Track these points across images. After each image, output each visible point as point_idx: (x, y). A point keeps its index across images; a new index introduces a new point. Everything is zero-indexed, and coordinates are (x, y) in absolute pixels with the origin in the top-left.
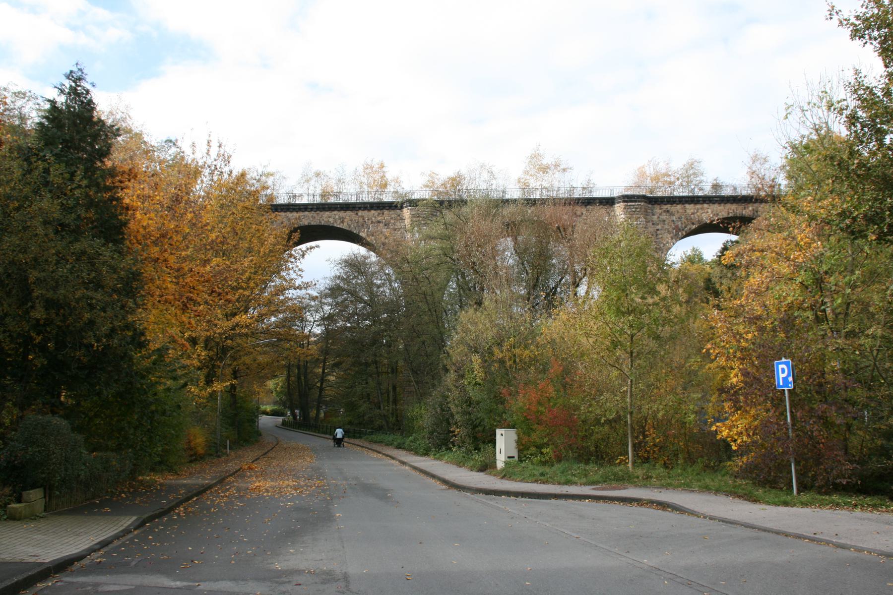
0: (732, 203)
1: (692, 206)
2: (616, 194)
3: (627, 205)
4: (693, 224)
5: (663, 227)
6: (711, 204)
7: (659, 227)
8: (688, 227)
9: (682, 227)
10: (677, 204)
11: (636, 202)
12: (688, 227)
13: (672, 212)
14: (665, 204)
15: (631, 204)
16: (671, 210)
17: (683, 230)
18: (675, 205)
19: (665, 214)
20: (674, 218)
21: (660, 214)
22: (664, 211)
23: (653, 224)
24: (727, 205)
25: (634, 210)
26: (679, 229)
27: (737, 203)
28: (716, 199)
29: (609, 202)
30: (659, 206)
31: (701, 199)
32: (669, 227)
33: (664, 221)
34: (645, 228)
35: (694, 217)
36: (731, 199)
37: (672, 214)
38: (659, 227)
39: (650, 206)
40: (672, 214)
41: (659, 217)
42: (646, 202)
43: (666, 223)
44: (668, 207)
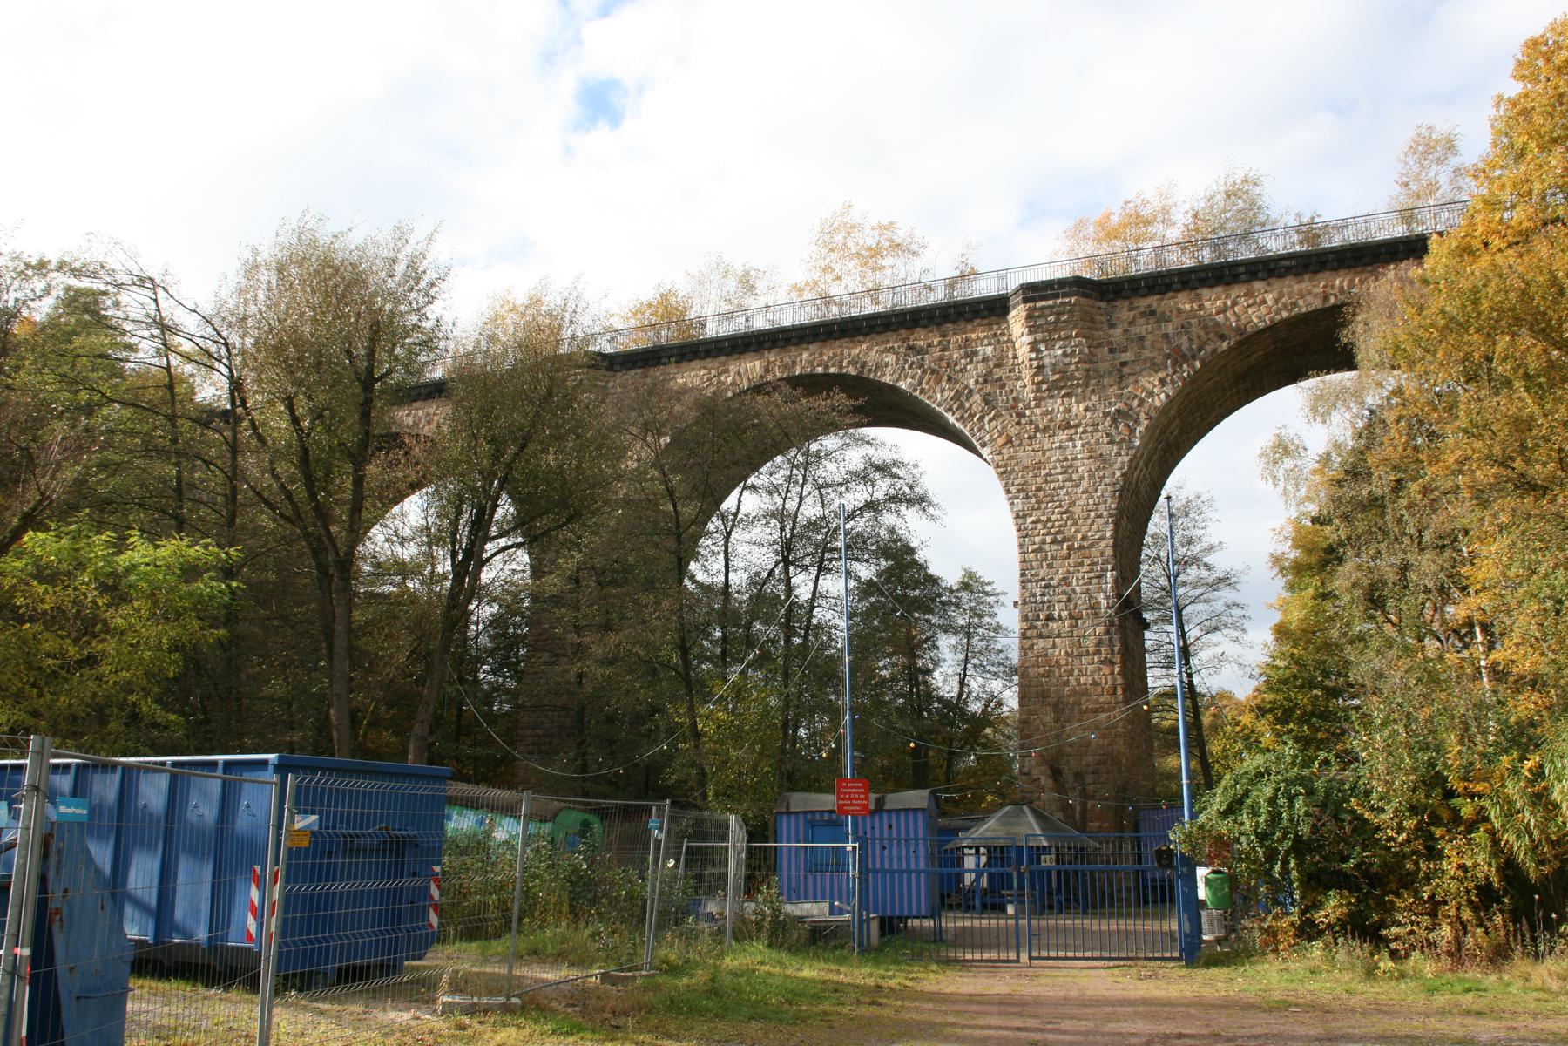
0: (1335, 270)
1: (1219, 289)
2: (1013, 283)
3: (1035, 309)
4: (1222, 337)
5: (1138, 356)
6: (1272, 280)
7: (1125, 357)
8: (1209, 348)
9: (1191, 349)
10: (1178, 291)
11: (1056, 296)
12: (1209, 348)
13: (1163, 313)
14: (1144, 296)
15: (1044, 303)
16: (1159, 311)
17: (1194, 357)
18: (1170, 294)
19: (1142, 321)
20: (1169, 329)
21: (1132, 323)
22: (1143, 314)
23: (1111, 351)
24: (1320, 275)
25: (1052, 318)
26: (1184, 356)
27: (1349, 267)
28: (1287, 263)
29: (995, 308)
30: (1127, 303)
31: (1242, 269)
32: (1155, 353)
33: (1141, 339)
34: (1091, 362)
35: (1227, 318)
36: (1331, 257)
37: (1163, 319)
38: (1125, 357)
39: (1103, 305)
40: (1163, 319)
41: (1126, 331)
42: (1084, 295)
43: (1147, 343)
44: (1153, 301)
